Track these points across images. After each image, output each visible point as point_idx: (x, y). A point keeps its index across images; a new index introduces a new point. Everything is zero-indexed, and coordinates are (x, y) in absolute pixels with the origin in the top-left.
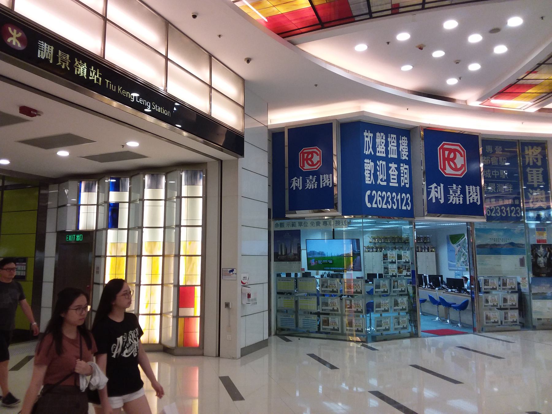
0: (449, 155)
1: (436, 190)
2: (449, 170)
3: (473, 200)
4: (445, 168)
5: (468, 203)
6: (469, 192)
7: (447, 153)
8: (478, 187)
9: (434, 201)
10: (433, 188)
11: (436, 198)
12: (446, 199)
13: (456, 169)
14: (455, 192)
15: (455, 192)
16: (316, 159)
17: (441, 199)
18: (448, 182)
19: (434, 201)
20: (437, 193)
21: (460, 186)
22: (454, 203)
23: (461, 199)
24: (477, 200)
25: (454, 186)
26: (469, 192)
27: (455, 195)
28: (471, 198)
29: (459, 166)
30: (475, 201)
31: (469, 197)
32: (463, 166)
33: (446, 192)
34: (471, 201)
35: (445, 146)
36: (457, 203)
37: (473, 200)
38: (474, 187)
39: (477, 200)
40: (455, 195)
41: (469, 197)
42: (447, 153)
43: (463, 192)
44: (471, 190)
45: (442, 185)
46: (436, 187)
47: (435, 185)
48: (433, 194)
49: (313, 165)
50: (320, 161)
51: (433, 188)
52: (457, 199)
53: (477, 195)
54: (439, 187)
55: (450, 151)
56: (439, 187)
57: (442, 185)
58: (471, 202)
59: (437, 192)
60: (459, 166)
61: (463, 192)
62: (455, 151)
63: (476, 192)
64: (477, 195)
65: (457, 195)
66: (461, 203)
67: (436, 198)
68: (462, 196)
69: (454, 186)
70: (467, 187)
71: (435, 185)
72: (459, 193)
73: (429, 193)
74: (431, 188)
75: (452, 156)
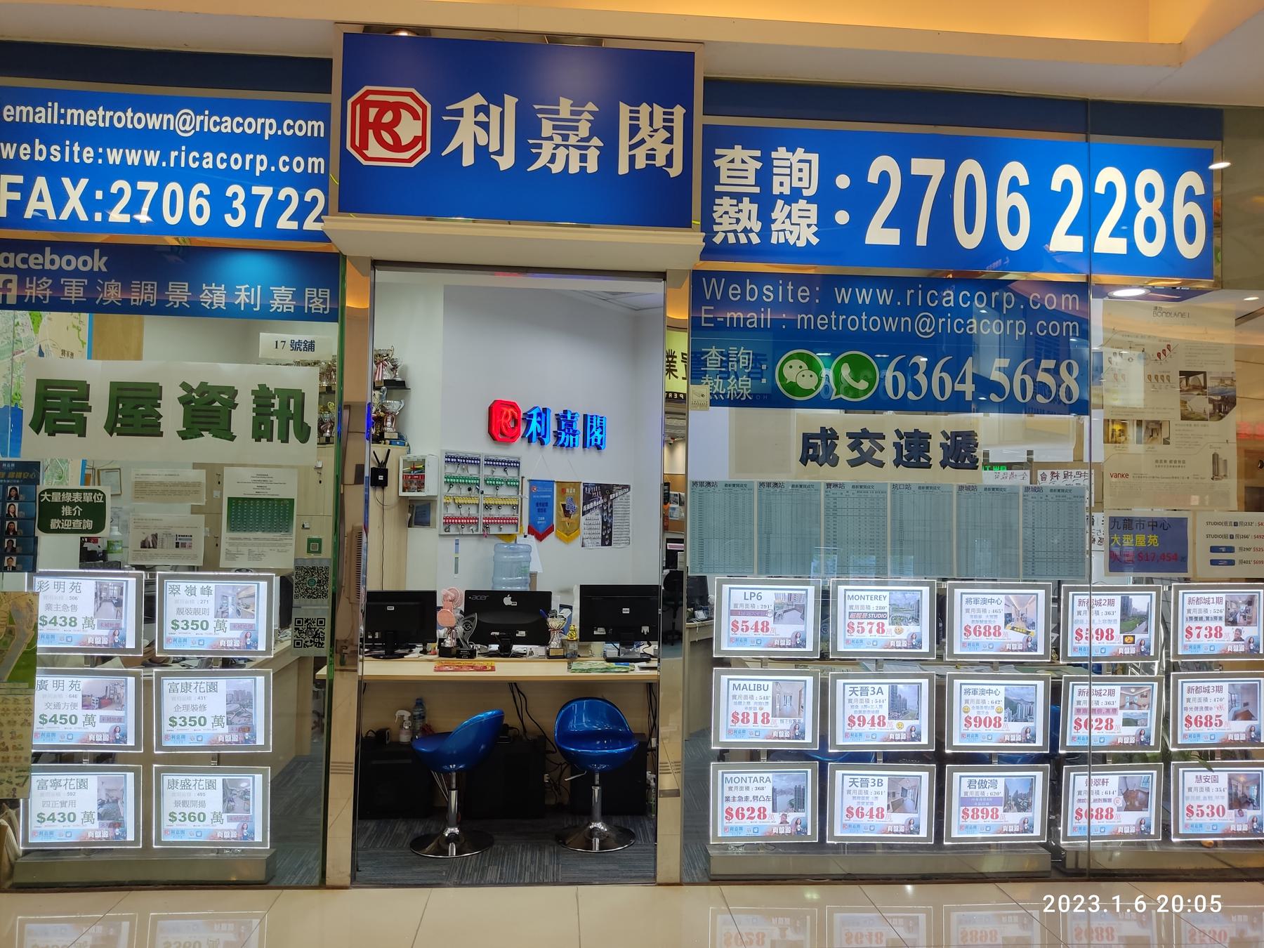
1: (482, 117)
3: (650, 157)
5: (623, 169)
8: (679, 111)
9: (468, 159)
12: (525, 154)
14: (565, 128)
15: (565, 128)
16: (408, 129)
17: (500, 152)
19: (468, 159)
21: (591, 107)
22: (557, 168)
23: (593, 155)
24: (670, 158)
26: (634, 130)
27: (565, 137)
28: (640, 153)
30: (660, 161)
31: (632, 147)
34: (641, 163)
37: (650, 157)
38: (659, 110)
39: (670, 158)
40: (565, 137)
41: (632, 147)
43: (605, 128)
44: (644, 122)
45: (510, 102)
46: (478, 109)
47: (478, 99)
48: (466, 137)
49: (397, 146)
50: (423, 138)
52: (575, 154)
53: (669, 141)
54: (495, 110)
56: (495, 110)
57: (510, 102)
59: (485, 126)
61: (605, 128)
63: (670, 130)
64: (669, 141)
65: (573, 140)
66: (592, 167)
67: (481, 151)
68: (596, 141)
70: (624, 109)
71: (478, 99)
74: (460, 113)
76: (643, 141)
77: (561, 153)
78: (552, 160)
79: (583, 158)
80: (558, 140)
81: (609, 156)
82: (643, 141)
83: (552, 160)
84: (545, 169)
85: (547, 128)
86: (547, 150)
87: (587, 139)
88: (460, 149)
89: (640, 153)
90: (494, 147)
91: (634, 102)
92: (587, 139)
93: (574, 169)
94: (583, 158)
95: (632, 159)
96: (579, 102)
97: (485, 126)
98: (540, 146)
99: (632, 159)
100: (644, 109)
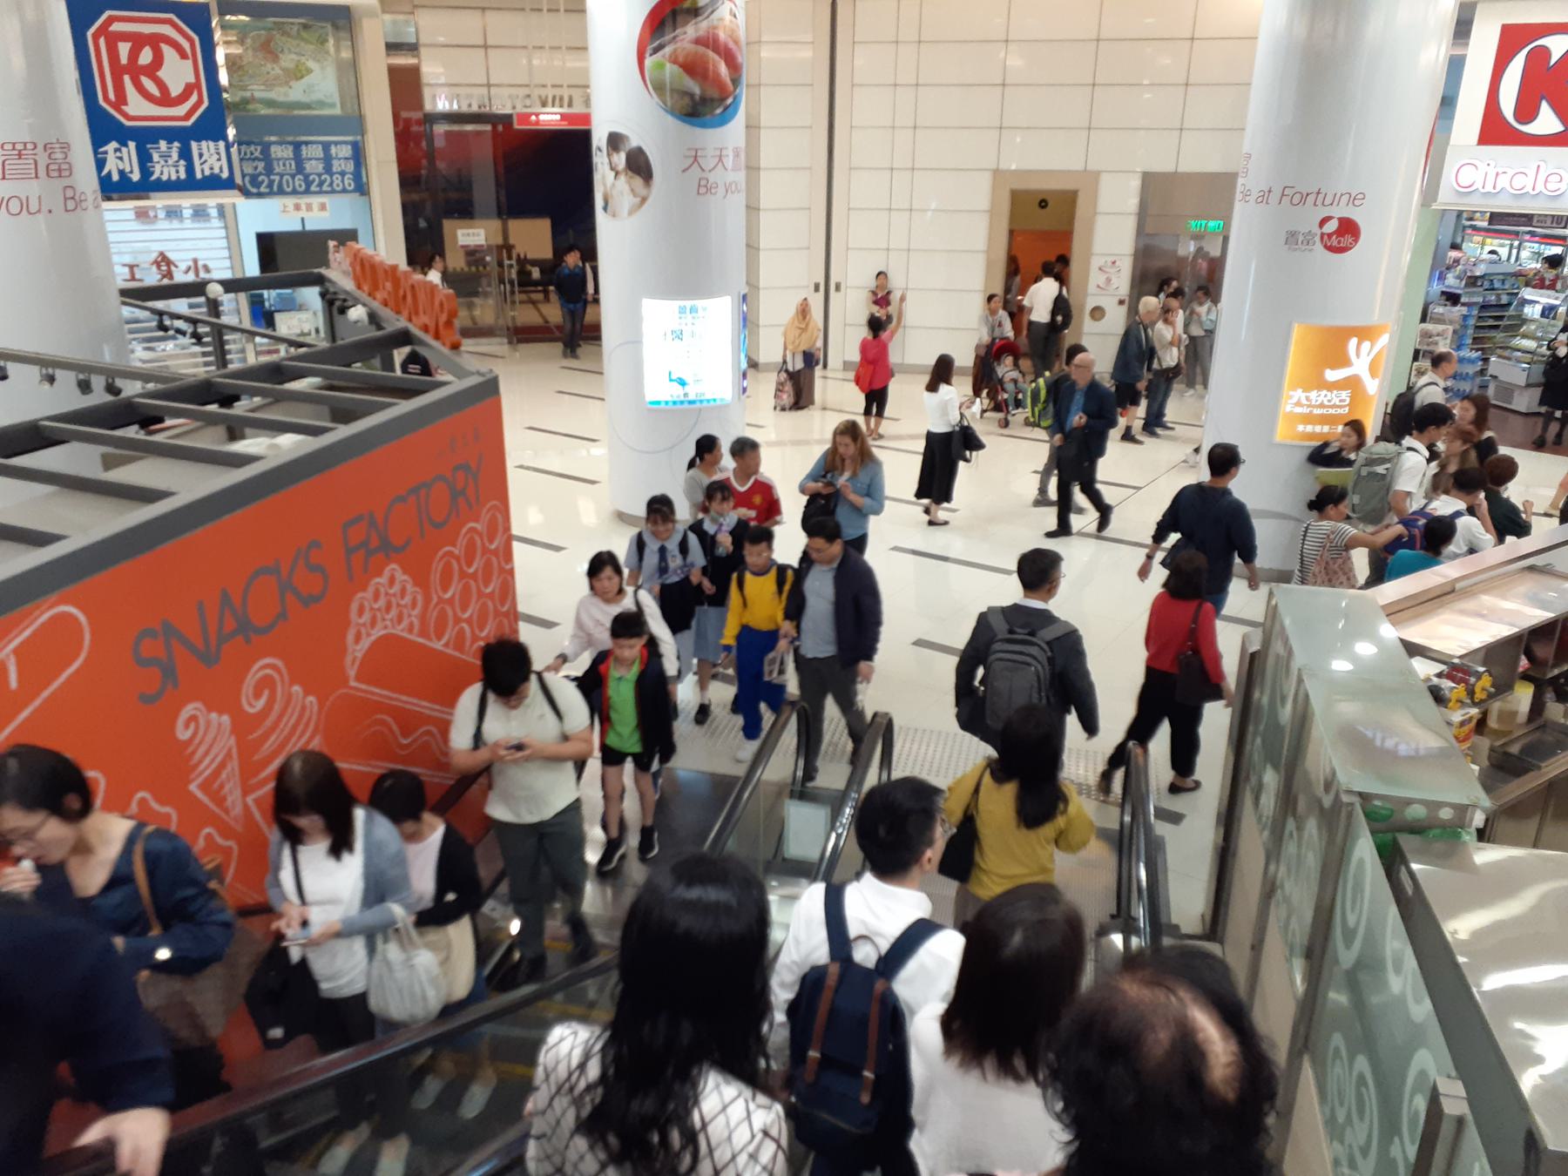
5: (199, 176)
6: (201, 155)
8: (222, 144)
9: (115, 177)
10: (111, 152)
11: (122, 173)
14: (165, 156)
15: (165, 156)
18: (145, 138)
19: (115, 177)
20: (121, 159)
22: (165, 178)
25: (163, 144)
26: (201, 155)
30: (216, 171)
33: (144, 159)
34: (207, 173)
38: (211, 144)
43: (185, 154)
45: (132, 145)
46: (116, 150)
48: (112, 166)
51: (111, 152)
52: (173, 170)
56: (124, 150)
59: (121, 159)
61: (185, 154)
66: (183, 176)
67: (122, 173)
68: (182, 162)
69: (163, 144)
71: (114, 144)
72: (175, 156)
73: (100, 164)
77: (166, 170)
81: (190, 169)
84: (159, 179)
85: (156, 157)
88: (109, 173)
89: (206, 167)
90: (128, 169)
91: (198, 140)
93: (174, 177)
96: (170, 142)
97: (121, 159)
100: (204, 143)
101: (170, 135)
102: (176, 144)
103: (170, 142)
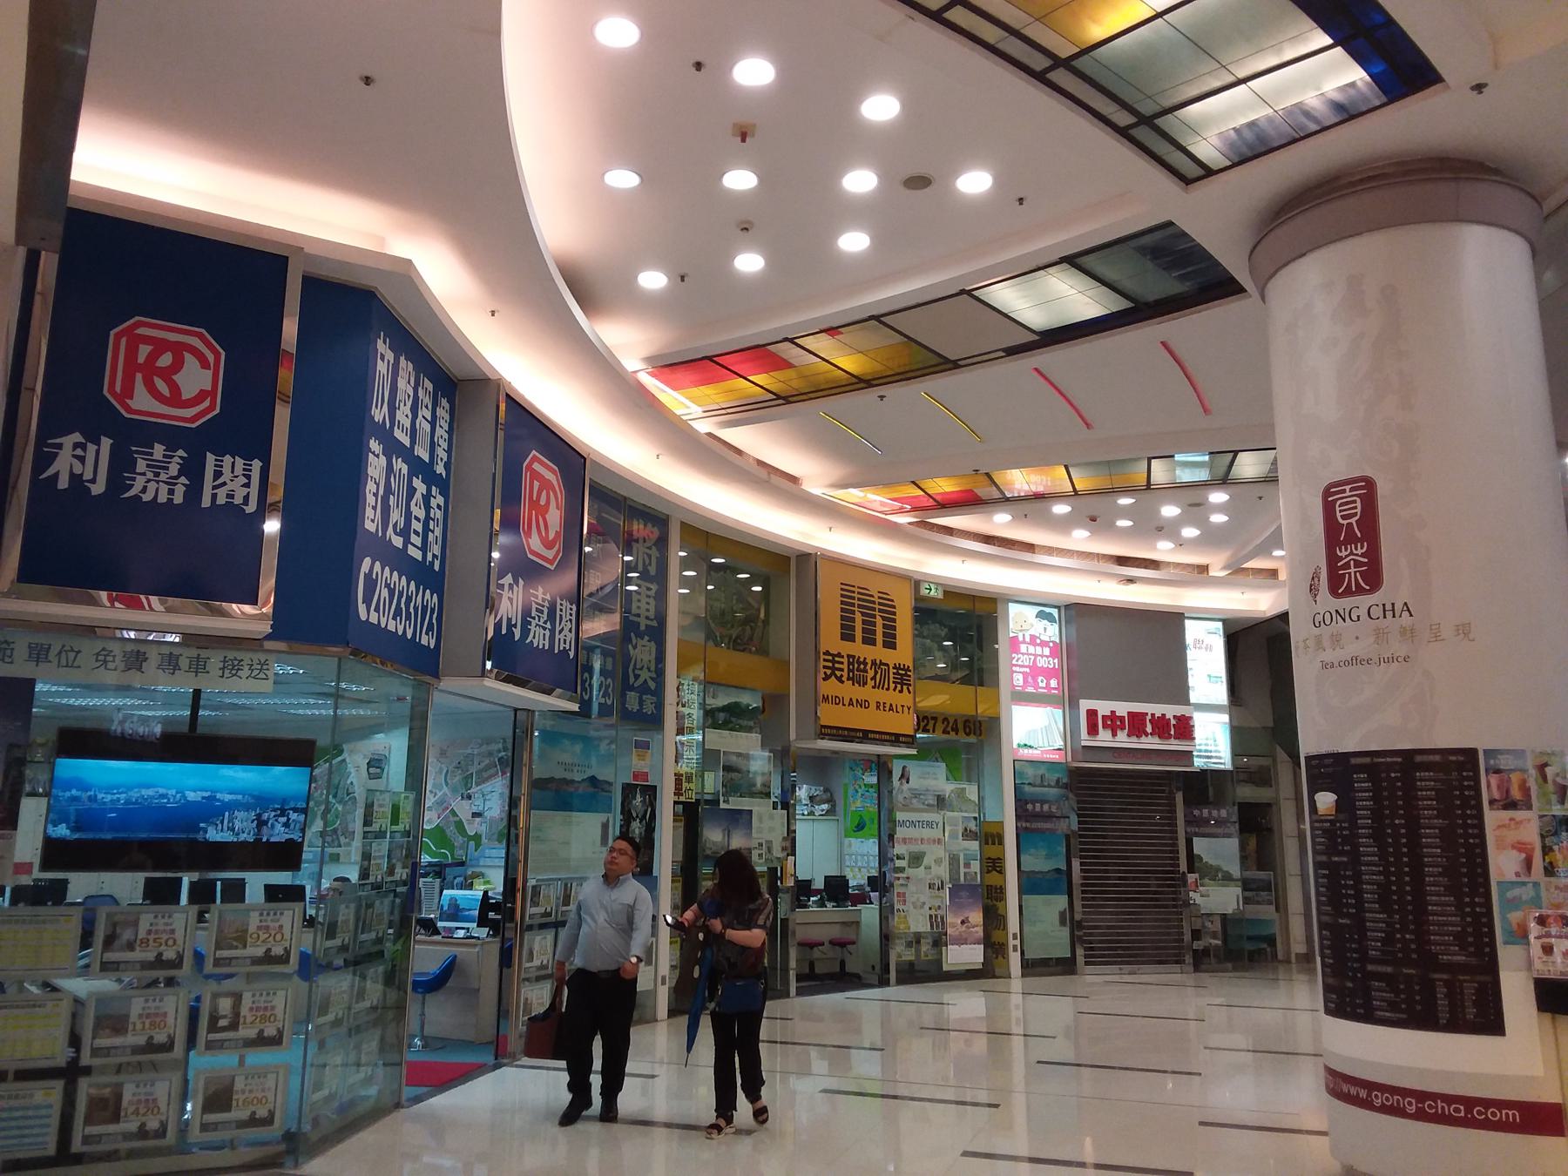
0: (153, 357)
2: (142, 402)
4: (128, 391)
5: (206, 502)
7: (144, 351)
8: (257, 464)
13: (175, 399)
14: (157, 467)
15: (157, 467)
18: (132, 436)
21: (181, 453)
23: (180, 491)
24: (246, 498)
25: (159, 450)
26: (217, 475)
29: (187, 394)
30: (238, 500)
31: (214, 488)
32: (202, 395)
33: (121, 465)
34: (221, 500)
35: (141, 331)
36: (162, 498)
38: (240, 462)
39: (246, 498)
41: (214, 488)
42: (144, 351)
43: (193, 471)
44: (226, 470)
52: (164, 489)
53: (247, 485)
55: (160, 346)
58: (221, 500)
60: (187, 394)
62: (179, 350)
63: (248, 477)
65: (163, 477)
66: (178, 499)
68: (183, 480)
69: (159, 450)
70: (210, 458)
72: (174, 469)
75: (165, 360)
76: (224, 484)
77: (152, 486)
78: (144, 490)
79: (171, 492)
80: (150, 475)
81: (194, 491)
82: (224, 484)
83: (144, 490)
85: (141, 465)
86: (140, 482)
87: (176, 478)
91: (220, 453)
92: (176, 478)
93: (162, 498)
94: (171, 492)
95: (214, 496)
96: (171, 448)
98: (134, 479)
99: (214, 496)
100: (228, 459)
101: (173, 437)
102: (181, 453)
103: (171, 448)
